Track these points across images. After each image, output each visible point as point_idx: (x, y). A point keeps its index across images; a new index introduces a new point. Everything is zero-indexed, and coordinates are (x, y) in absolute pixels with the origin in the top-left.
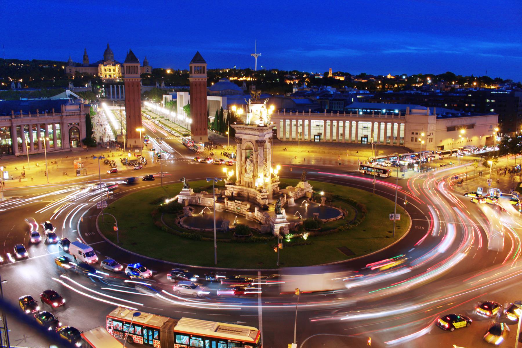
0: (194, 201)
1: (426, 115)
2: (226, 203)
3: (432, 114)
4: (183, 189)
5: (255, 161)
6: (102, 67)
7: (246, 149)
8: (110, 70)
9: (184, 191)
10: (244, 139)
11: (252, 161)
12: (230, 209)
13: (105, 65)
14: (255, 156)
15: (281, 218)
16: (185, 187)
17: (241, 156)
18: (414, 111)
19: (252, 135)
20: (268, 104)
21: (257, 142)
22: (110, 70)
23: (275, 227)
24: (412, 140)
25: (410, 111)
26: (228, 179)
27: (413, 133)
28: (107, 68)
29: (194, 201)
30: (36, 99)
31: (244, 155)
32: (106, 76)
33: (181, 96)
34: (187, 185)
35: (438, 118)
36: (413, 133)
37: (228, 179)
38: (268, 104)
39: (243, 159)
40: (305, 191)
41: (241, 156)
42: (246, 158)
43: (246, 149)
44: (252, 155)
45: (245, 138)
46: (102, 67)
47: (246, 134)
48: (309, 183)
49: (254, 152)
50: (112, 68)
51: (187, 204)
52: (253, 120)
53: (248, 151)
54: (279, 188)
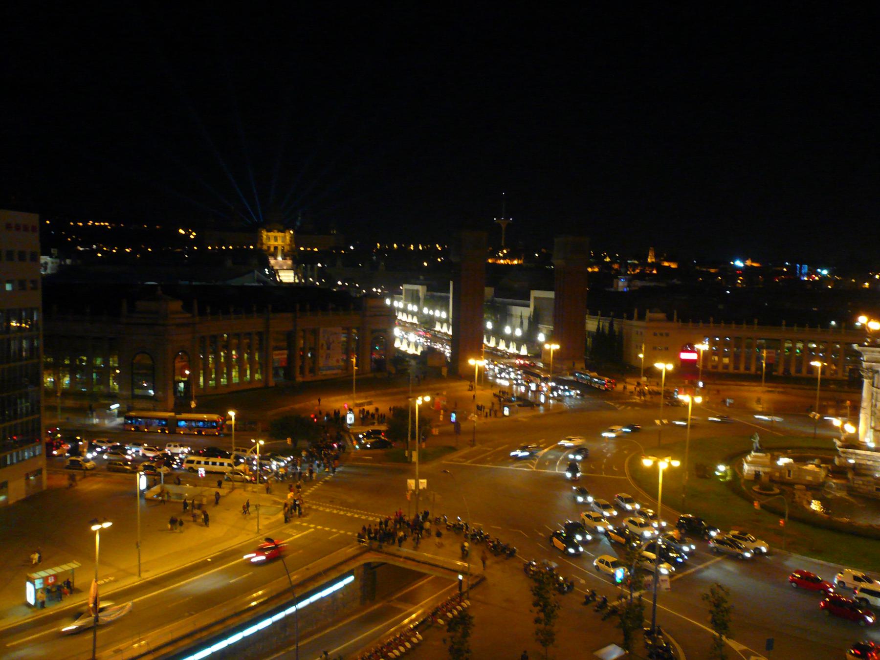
0: (777, 474)
4: (753, 453)
6: (265, 234)
8: (276, 239)
9: (755, 457)
13: (268, 231)
16: (757, 451)
22: (276, 239)
26: (843, 438)
28: (271, 234)
29: (777, 474)
30: (204, 283)
32: (269, 247)
34: (760, 446)
46: (265, 234)
50: (281, 234)
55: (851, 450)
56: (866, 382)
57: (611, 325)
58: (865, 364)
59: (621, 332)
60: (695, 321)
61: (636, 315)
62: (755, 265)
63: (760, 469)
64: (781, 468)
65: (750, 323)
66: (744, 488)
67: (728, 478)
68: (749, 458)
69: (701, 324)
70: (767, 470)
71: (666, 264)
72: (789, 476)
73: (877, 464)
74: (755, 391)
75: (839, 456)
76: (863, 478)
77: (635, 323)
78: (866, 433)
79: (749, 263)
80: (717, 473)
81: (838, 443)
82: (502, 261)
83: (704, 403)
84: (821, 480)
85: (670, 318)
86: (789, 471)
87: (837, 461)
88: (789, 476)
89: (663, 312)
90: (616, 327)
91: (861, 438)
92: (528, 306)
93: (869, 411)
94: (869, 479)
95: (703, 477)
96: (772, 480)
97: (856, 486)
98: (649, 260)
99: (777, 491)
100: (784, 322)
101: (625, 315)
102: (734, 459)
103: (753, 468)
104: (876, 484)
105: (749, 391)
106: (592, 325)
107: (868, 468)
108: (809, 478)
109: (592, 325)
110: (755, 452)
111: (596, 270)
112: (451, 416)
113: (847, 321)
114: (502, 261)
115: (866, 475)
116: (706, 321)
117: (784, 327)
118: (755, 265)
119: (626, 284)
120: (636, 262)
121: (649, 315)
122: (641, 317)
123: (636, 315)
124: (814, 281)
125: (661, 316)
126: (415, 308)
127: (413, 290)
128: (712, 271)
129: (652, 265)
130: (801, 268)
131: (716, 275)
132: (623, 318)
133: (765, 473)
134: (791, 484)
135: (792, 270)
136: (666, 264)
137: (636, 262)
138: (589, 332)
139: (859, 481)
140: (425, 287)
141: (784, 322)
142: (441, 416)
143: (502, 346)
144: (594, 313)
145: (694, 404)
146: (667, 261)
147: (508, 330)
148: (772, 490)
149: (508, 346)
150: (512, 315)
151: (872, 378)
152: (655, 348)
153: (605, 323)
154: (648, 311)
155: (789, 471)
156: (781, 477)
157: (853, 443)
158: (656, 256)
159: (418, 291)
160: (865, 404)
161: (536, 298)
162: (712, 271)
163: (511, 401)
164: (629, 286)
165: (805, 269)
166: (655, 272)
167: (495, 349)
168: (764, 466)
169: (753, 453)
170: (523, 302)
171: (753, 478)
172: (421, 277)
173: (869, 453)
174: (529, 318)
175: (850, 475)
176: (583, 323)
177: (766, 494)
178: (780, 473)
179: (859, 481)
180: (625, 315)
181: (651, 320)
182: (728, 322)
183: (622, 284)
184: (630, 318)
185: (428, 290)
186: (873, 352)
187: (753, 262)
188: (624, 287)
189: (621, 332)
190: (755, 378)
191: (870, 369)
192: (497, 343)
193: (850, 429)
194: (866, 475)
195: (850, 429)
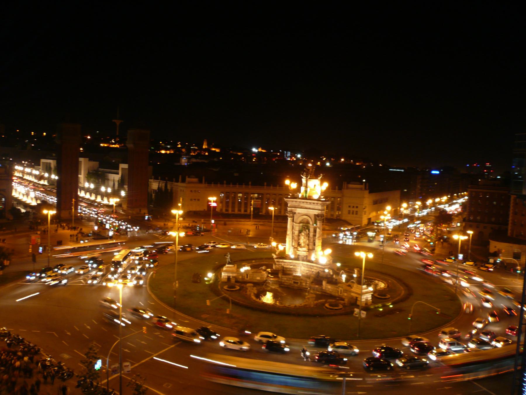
0: (240, 277)
1: (361, 189)
3: (366, 189)
4: (227, 265)
5: (311, 234)
7: (300, 223)
10: (299, 213)
11: (308, 235)
12: (286, 284)
14: (312, 230)
16: (229, 263)
18: (351, 186)
19: (310, 209)
20: (322, 181)
23: (363, 297)
25: (347, 186)
26: (277, 253)
27: (350, 206)
34: (231, 260)
35: (370, 192)
36: (350, 206)
37: (277, 253)
38: (322, 181)
39: (296, 233)
42: (300, 232)
43: (300, 223)
45: (300, 212)
47: (301, 208)
51: (233, 281)
52: (310, 195)
53: (301, 224)
55: (281, 260)
56: (289, 219)
57: (166, 186)
58: (289, 209)
59: (172, 190)
60: (216, 183)
61: (180, 179)
62: (263, 151)
63: (231, 275)
64: (242, 274)
65: (247, 184)
66: (219, 287)
67: (211, 282)
68: (224, 269)
69: (219, 185)
70: (234, 275)
71: (213, 149)
73: (295, 267)
74: (248, 225)
75: (275, 264)
76: (287, 277)
77: (180, 184)
78: (289, 249)
79: (260, 150)
80: (206, 279)
81: (275, 256)
82: (113, 146)
83: (187, 235)
84: (265, 279)
85: (200, 182)
86: (247, 275)
87: (274, 267)
89: (196, 178)
90: (169, 187)
91: (287, 253)
92: (118, 174)
93: (291, 237)
94: (290, 277)
95: (196, 282)
96: (237, 282)
97: (283, 281)
98: (204, 147)
99: (238, 288)
100: (265, 184)
101: (174, 179)
102: (217, 269)
103: (226, 274)
104: (294, 279)
105: (244, 225)
106: (155, 185)
107: (290, 270)
109: (155, 185)
110: (228, 264)
111: (172, 152)
112: (39, 249)
113: (278, 182)
114: (113, 146)
115: (289, 274)
116: (222, 183)
117: (265, 187)
118: (263, 151)
119: (186, 161)
120: (196, 148)
121: (188, 179)
122: (183, 181)
123: (180, 179)
124: (293, 160)
125: (196, 180)
126: (46, 175)
127: (47, 163)
128: (239, 154)
129: (205, 150)
130: (287, 154)
131: (241, 156)
133: (233, 277)
134: (246, 283)
135: (282, 154)
136: (213, 149)
137: (196, 148)
138: (154, 190)
139: (285, 278)
140: (55, 161)
141: (265, 184)
142: (30, 249)
143: (99, 199)
144: (156, 178)
145: (179, 237)
146: (215, 148)
147: (103, 189)
148: (235, 288)
149: (102, 199)
150: (108, 180)
151: (293, 217)
152: (191, 200)
153: (162, 185)
154: (187, 177)
155: (247, 275)
156: (243, 279)
157: (283, 256)
158: (208, 145)
159: (50, 163)
160: (289, 232)
161: (122, 169)
162: (239, 154)
163: (89, 236)
164: (188, 162)
165: (289, 154)
166: (207, 154)
167: (94, 201)
168: (232, 272)
169: (227, 265)
170: (116, 171)
171: (226, 280)
172: (54, 155)
173: (290, 261)
174: (118, 181)
175: (280, 275)
176: (147, 185)
177: (231, 291)
178: (242, 276)
179: (285, 278)
180: (174, 179)
181: (189, 183)
182: (241, 184)
183: (184, 161)
184: (177, 181)
186: (293, 201)
187: (262, 149)
188: (185, 162)
189: (172, 190)
190: (246, 217)
191: (291, 212)
192: (96, 198)
193: (281, 247)
194: (289, 274)
195: (281, 247)
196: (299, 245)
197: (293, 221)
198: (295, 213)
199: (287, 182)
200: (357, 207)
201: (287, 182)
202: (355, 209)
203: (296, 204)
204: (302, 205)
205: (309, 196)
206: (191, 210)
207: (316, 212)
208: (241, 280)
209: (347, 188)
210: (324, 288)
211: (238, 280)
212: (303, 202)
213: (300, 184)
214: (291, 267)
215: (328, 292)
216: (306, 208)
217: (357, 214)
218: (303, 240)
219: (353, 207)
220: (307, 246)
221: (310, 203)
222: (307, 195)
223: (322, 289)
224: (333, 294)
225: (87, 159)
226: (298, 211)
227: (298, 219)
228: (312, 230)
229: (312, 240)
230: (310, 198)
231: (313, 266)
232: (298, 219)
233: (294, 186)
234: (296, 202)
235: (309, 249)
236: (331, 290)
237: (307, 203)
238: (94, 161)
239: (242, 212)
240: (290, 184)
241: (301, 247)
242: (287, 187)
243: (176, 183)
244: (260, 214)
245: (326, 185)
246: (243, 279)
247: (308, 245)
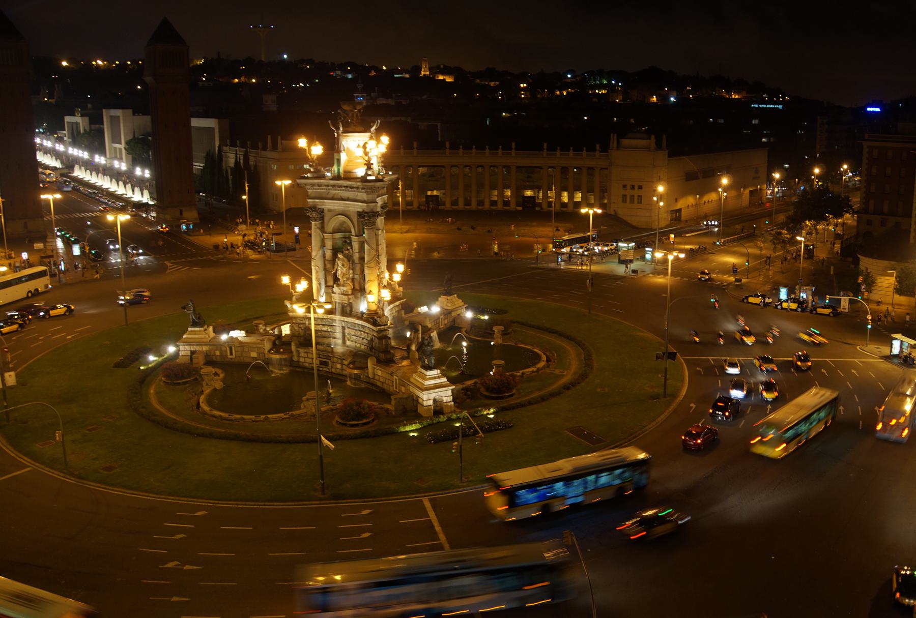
0: (218, 353)
2: (295, 353)
4: (190, 329)
5: (356, 256)
7: (334, 232)
10: (330, 210)
11: (349, 258)
14: (356, 246)
15: (435, 378)
16: (195, 324)
17: (323, 245)
18: (625, 142)
19: (348, 200)
21: (361, 215)
24: (624, 201)
25: (618, 142)
29: (218, 353)
31: (329, 244)
33: (114, 121)
39: (329, 254)
40: (453, 314)
41: (323, 245)
42: (336, 251)
43: (334, 232)
44: (350, 244)
47: (333, 199)
48: (459, 297)
49: (354, 238)
51: (200, 360)
52: (349, 168)
53: (339, 235)
54: (403, 312)
59: (256, 166)
63: (197, 348)
64: (220, 345)
70: (205, 348)
72: (231, 354)
77: (269, 154)
86: (231, 348)
88: (231, 354)
103: (188, 348)
108: (254, 355)
109: (231, 160)
128: (492, 84)
131: (496, 89)
132: (257, 148)
136: (441, 77)
146: (443, 74)
151: (322, 218)
155: (231, 348)
158: (430, 70)
159: (77, 124)
168: (200, 343)
178: (221, 351)
184: (265, 149)
185: (91, 123)
186: (313, 185)
189: (256, 166)
191: (314, 208)
196: (336, 279)
197: (322, 229)
198: (323, 211)
199: (302, 142)
200: (640, 187)
201: (302, 142)
202: (636, 192)
203: (323, 191)
204: (333, 192)
205: (346, 172)
206: (293, 206)
207: (359, 207)
208: (218, 359)
209: (619, 146)
210: (371, 376)
211: (214, 358)
212: (334, 186)
213: (333, 148)
214: (325, 328)
215: (379, 384)
216: (342, 199)
217: (640, 202)
218: (341, 269)
219: (633, 187)
220: (349, 282)
221: (346, 187)
222: (341, 170)
223: (368, 377)
224: (386, 387)
225: (130, 111)
226: (328, 205)
227: (331, 225)
228: (356, 246)
229: (358, 267)
230: (348, 176)
231: (363, 327)
232: (331, 225)
233: (317, 150)
234: (319, 185)
235: (354, 289)
236: (382, 380)
237: (340, 186)
238: (144, 114)
239: (474, 205)
240: (309, 146)
241: (338, 285)
242: (303, 151)
243: (263, 153)
244: (441, 207)
245: (385, 139)
246: (223, 355)
247: (353, 280)
